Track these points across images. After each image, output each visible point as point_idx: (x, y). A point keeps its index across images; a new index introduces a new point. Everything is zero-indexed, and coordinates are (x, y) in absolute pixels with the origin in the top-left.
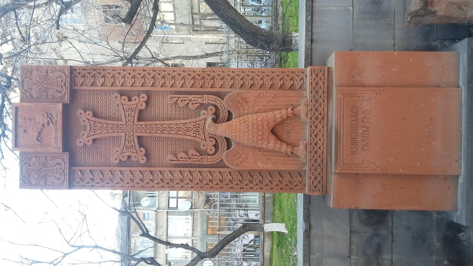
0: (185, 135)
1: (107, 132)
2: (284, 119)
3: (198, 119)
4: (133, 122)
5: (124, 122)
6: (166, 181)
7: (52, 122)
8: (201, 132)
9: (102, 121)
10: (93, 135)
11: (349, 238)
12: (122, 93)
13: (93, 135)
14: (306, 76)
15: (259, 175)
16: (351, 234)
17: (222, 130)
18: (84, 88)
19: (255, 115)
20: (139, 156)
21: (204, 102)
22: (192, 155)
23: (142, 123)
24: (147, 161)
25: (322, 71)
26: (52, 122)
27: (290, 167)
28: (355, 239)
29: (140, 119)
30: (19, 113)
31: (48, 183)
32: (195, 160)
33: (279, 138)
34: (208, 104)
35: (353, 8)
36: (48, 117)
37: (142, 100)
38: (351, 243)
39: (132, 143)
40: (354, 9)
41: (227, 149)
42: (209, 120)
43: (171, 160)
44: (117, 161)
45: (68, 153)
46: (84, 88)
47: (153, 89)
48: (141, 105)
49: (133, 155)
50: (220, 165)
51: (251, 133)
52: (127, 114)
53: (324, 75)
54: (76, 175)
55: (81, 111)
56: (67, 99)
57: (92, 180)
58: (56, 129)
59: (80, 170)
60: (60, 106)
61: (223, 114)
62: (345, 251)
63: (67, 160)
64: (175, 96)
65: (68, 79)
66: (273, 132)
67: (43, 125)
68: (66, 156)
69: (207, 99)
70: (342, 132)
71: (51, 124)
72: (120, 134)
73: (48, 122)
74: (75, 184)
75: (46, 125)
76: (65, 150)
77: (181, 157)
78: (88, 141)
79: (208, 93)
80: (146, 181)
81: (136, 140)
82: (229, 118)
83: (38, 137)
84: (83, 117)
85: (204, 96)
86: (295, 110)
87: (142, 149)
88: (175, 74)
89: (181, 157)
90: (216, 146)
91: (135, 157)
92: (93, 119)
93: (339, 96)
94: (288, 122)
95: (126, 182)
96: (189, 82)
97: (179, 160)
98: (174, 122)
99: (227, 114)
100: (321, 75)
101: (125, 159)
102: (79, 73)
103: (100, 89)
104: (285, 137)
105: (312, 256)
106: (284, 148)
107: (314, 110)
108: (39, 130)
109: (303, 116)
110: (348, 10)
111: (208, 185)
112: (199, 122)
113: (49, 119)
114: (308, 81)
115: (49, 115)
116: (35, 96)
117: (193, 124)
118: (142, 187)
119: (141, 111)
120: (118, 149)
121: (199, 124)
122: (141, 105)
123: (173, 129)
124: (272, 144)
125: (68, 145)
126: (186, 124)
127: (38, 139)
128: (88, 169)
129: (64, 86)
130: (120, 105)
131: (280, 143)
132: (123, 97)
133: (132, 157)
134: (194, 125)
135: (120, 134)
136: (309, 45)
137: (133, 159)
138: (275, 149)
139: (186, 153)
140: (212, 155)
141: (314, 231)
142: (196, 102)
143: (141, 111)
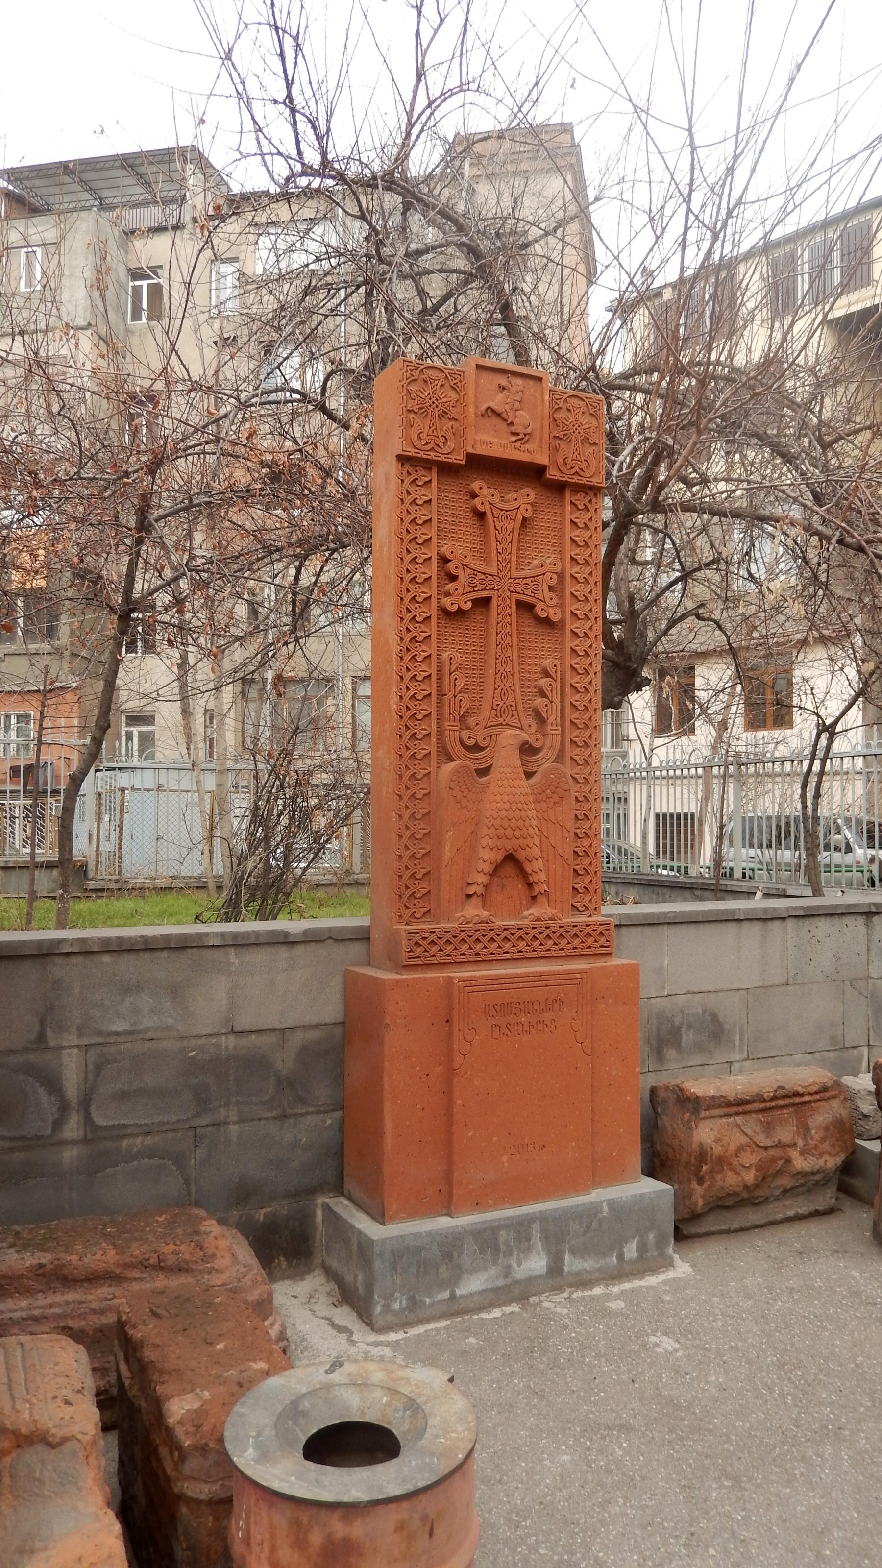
3: (522, 713)
5: (515, 574)
8: (501, 720)
9: (516, 533)
11: (271, 1027)
12: (561, 576)
15: (425, 831)
20: (459, 597)
21: (550, 727)
23: (514, 607)
25: (607, 944)
26: (516, 441)
29: (520, 604)
31: (412, 415)
33: (497, 870)
39: (479, 587)
45: (464, 462)
46: (568, 507)
47: (568, 633)
51: (510, 814)
52: (528, 581)
53: (602, 946)
54: (422, 472)
56: (552, 474)
57: (414, 502)
58: (505, 446)
59: (430, 481)
60: (542, 459)
62: (244, 1022)
64: (559, 673)
65: (584, 481)
67: (512, 424)
68: (459, 458)
71: (513, 438)
73: (518, 434)
74: (407, 467)
76: (470, 457)
80: (412, 607)
81: (484, 594)
83: (493, 411)
84: (523, 498)
87: (470, 604)
88: (592, 674)
92: (520, 518)
93: (578, 975)
102: (590, 501)
105: (232, 951)
107: (548, 932)
108: (504, 415)
109: (534, 911)
110: (664, 988)
114: (582, 919)
116: (557, 415)
119: (530, 607)
125: (480, 464)
129: (573, 471)
130: (542, 570)
135: (495, 564)
141: (284, 952)
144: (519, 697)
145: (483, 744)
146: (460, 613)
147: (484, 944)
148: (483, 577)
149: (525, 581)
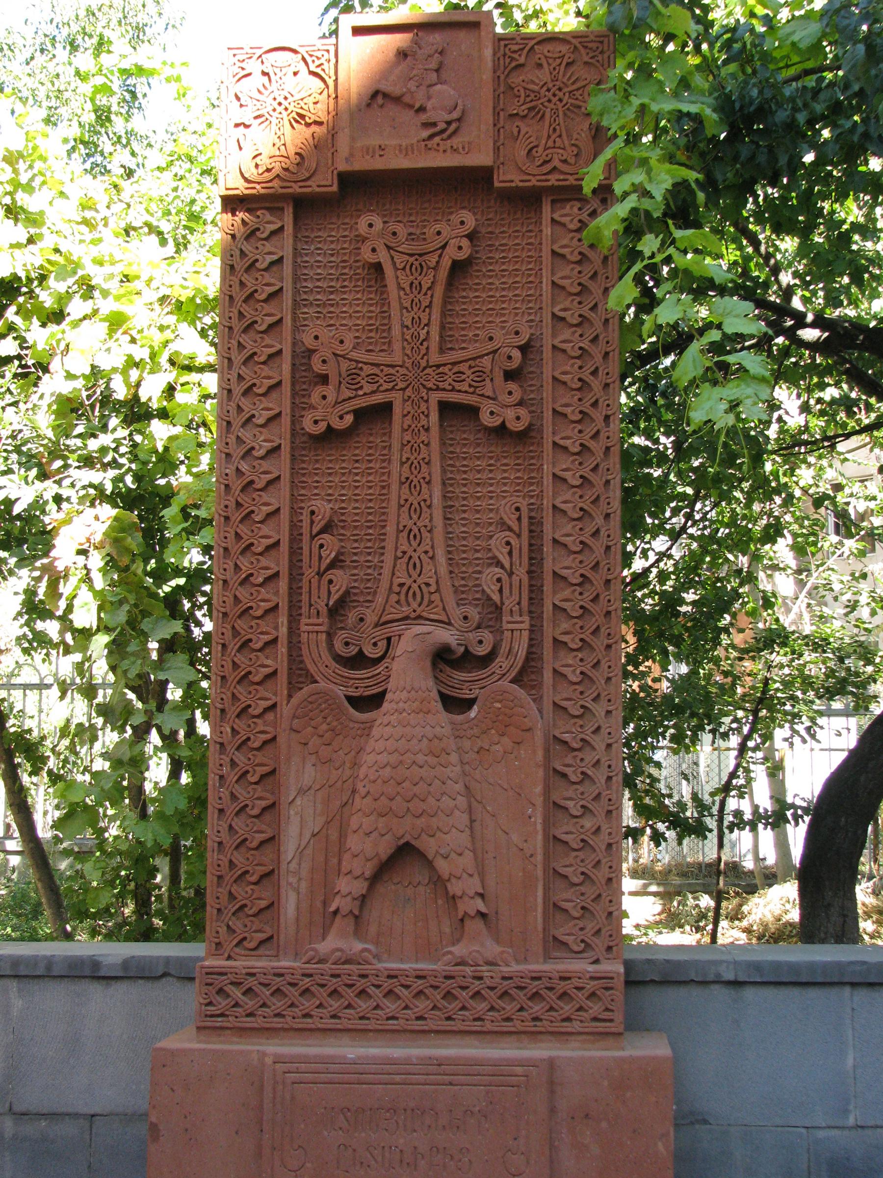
0: (396, 558)
1: (403, 308)
2: (449, 885)
4: (438, 389)
5: (435, 358)
6: (244, 499)
7: (431, 137)
9: (439, 291)
10: (394, 263)
11: (70, 1110)
13: (394, 263)
14: (597, 961)
15: (264, 803)
16: (84, 1115)
17: (407, 676)
18: (547, 231)
19: (459, 787)
20: (327, 409)
22: (330, 582)
23: (434, 417)
24: (311, 436)
26: (431, 137)
27: (290, 906)
28: (68, 1129)
29: (445, 407)
30: (462, 34)
32: (314, 592)
33: (385, 869)
34: (498, 631)
35: (850, 1128)
36: (449, 123)
37: (510, 414)
38: (53, 1116)
39: (368, 388)
40: (846, 1132)
41: (349, 699)
42: (446, 636)
43: (313, 513)
44: (308, 341)
45: (335, 188)
46: (547, 231)
48: (492, 413)
49: (330, 391)
50: (299, 675)
52: (463, 367)
53: (595, 1019)
55: (471, 221)
56: (508, 177)
58: (406, 151)
59: (282, 228)
60: (481, 158)
61: (462, 681)
62: (31, 1098)
63: (313, 187)
64: (525, 521)
66: (405, 853)
67: (422, 109)
69: (515, 627)
70: (398, 1078)
72: (397, 346)
73: (434, 124)
75: (423, 117)
77: (322, 546)
78: (374, 250)
79: (535, 631)
82: (454, 704)
83: (386, 95)
84: (452, 228)
85: (526, 618)
86: (479, 924)
87: (349, 419)
89: (322, 546)
90: (359, 661)
91: (324, 397)
92: (446, 263)
93: (519, 1070)
94: (440, 902)
95: (244, 371)
96: (568, 566)
97: (313, 538)
98: (438, 521)
99: (467, 694)
100: (596, 1008)
101: (318, 367)
103: (544, 280)
104: (381, 889)
106: (349, 887)
107: (477, 985)
108: (407, 99)
110: (846, 1112)
111: (234, 637)
112: (438, 602)
113: (444, 126)
114: (580, 966)
115: (454, 126)
116: (516, 79)
117: (432, 581)
118: (229, 423)
119: (473, 411)
120: (348, 344)
121: (431, 602)
122: (492, 413)
123: (415, 517)
124: (366, 846)
126: (432, 558)
127: (380, 100)
128: (287, 252)
129: (548, 167)
130: (490, 346)
131: (368, 874)
132: (517, 354)
133: (324, 388)
134: (428, 585)
136: (718, 975)
137: (319, 390)
138: (347, 856)
139: (332, 565)
140: (331, 646)
141: (95, 990)
142: (506, 592)
143: (473, 411)
144: (443, 570)
145: (370, 652)
146: (330, 436)
147: (343, 997)
148: (376, 370)
149: (456, 369)
